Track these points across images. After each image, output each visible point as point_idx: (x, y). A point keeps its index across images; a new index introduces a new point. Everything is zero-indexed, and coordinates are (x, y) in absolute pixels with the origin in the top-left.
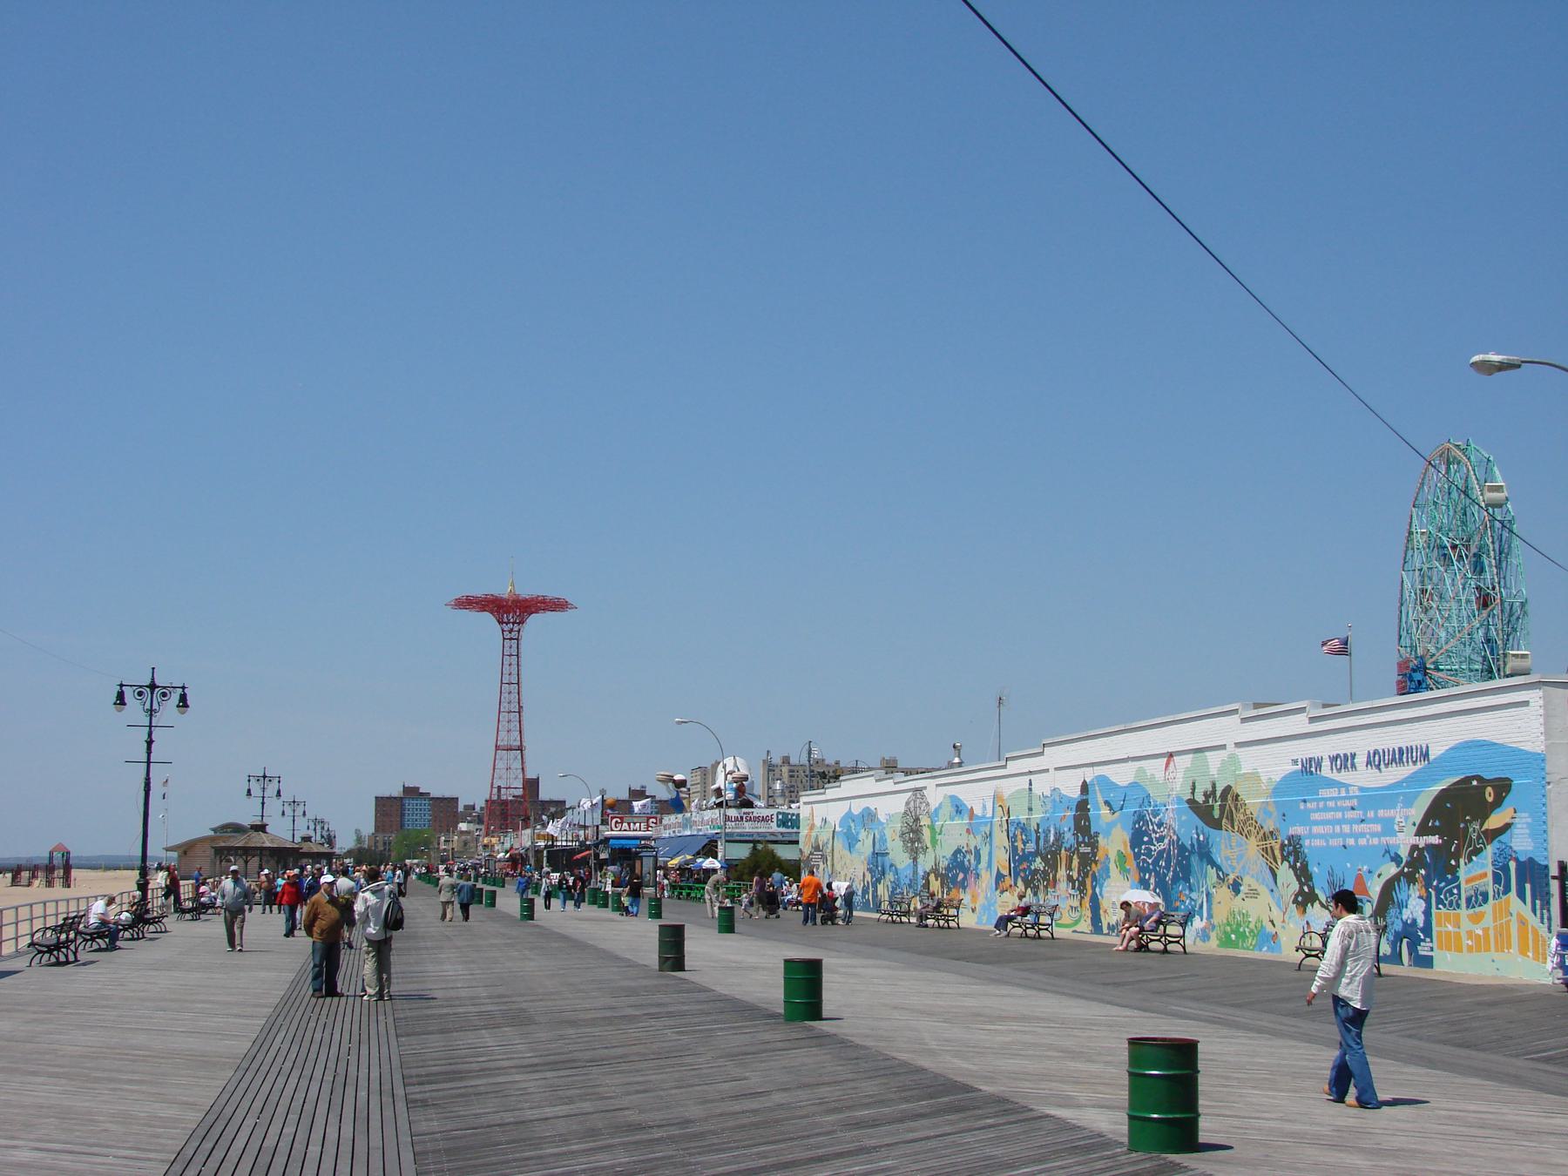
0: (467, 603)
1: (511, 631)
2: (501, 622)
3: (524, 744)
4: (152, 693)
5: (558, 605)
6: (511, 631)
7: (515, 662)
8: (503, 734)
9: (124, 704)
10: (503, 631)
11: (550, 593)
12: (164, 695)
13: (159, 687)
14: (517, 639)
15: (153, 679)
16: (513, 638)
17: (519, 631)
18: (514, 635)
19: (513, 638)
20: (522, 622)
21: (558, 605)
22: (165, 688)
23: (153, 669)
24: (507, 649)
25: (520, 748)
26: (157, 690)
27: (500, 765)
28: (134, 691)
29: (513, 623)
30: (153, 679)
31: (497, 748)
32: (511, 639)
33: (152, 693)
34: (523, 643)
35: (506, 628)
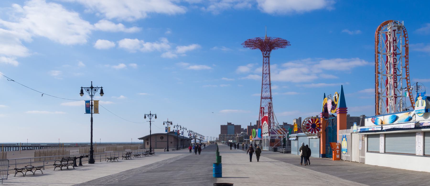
2: (262, 51)
3: (272, 96)
4: (92, 90)
8: (263, 93)
9: (83, 94)
10: (263, 54)
12: (95, 90)
13: (94, 88)
14: (269, 57)
15: (92, 85)
17: (269, 54)
20: (270, 51)
22: (96, 88)
23: (92, 82)
26: (93, 89)
28: (86, 90)
29: (267, 51)
30: (92, 85)
31: (262, 98)
32: (266, 57)
33: (92, 90)
34: (270, 58)
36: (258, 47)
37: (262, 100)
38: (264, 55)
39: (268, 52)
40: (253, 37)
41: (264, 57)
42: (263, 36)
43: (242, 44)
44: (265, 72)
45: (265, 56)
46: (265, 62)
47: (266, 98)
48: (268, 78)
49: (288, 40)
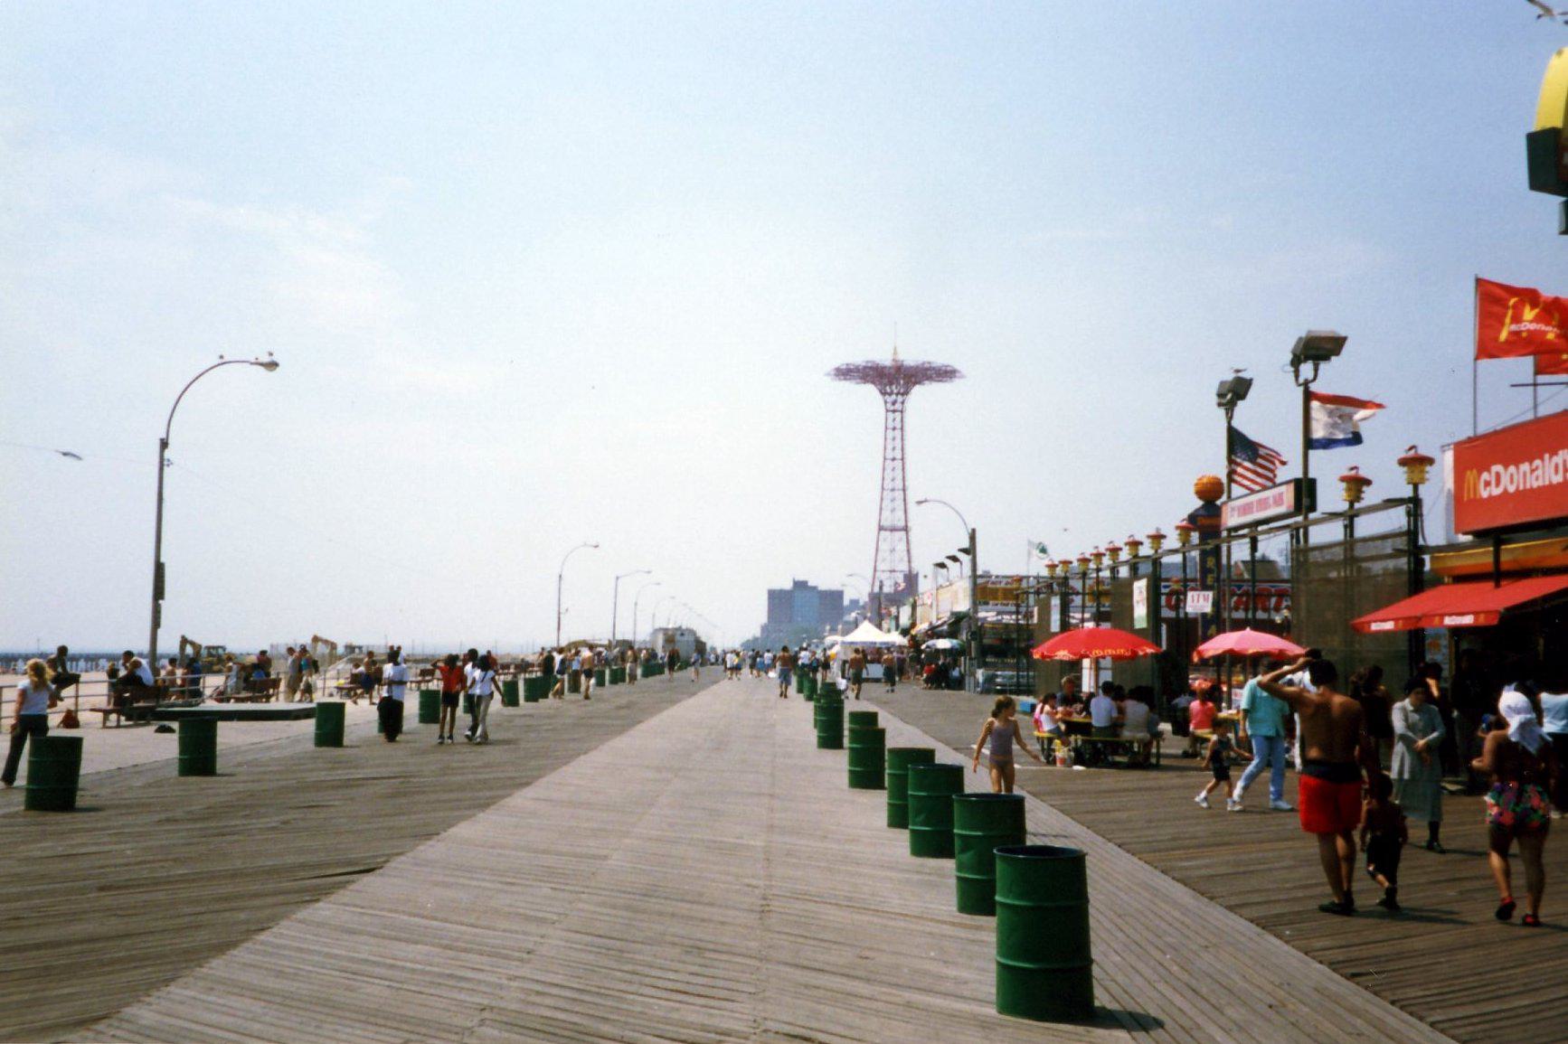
0: (845, 373)
1: (894, 403)
2: (884, 393)
3: (909, 525)
5: (944, 374)
6: (894, 403)
7: (899, 437)
8: (886, 513)
10: (886, 402)
11: (939, 360)
14: (902, 412)
16: (896, 410)
17: (903, 403)
18: (898, 406)
19: (896, 410)
20: (906, 393)
21: (944, 374)
24: (890, 421)
25: (906, 529)
27: (884, 546)
29: (897, 394)
31: (881, 528)
32: (894, 411)
35: (890, 399)
36: (873, 382)
37: (882, 533)
38: (889, 405)
39: (900, 398)
40: (859, 358)
41: (887, 411)
42: (884, 358)
43: (828, 374)
44: (890, 455)
45: (892, 408)
46: (891, 425)
47: (893, 529)
48: (899, 473)
49: (957, 366)
